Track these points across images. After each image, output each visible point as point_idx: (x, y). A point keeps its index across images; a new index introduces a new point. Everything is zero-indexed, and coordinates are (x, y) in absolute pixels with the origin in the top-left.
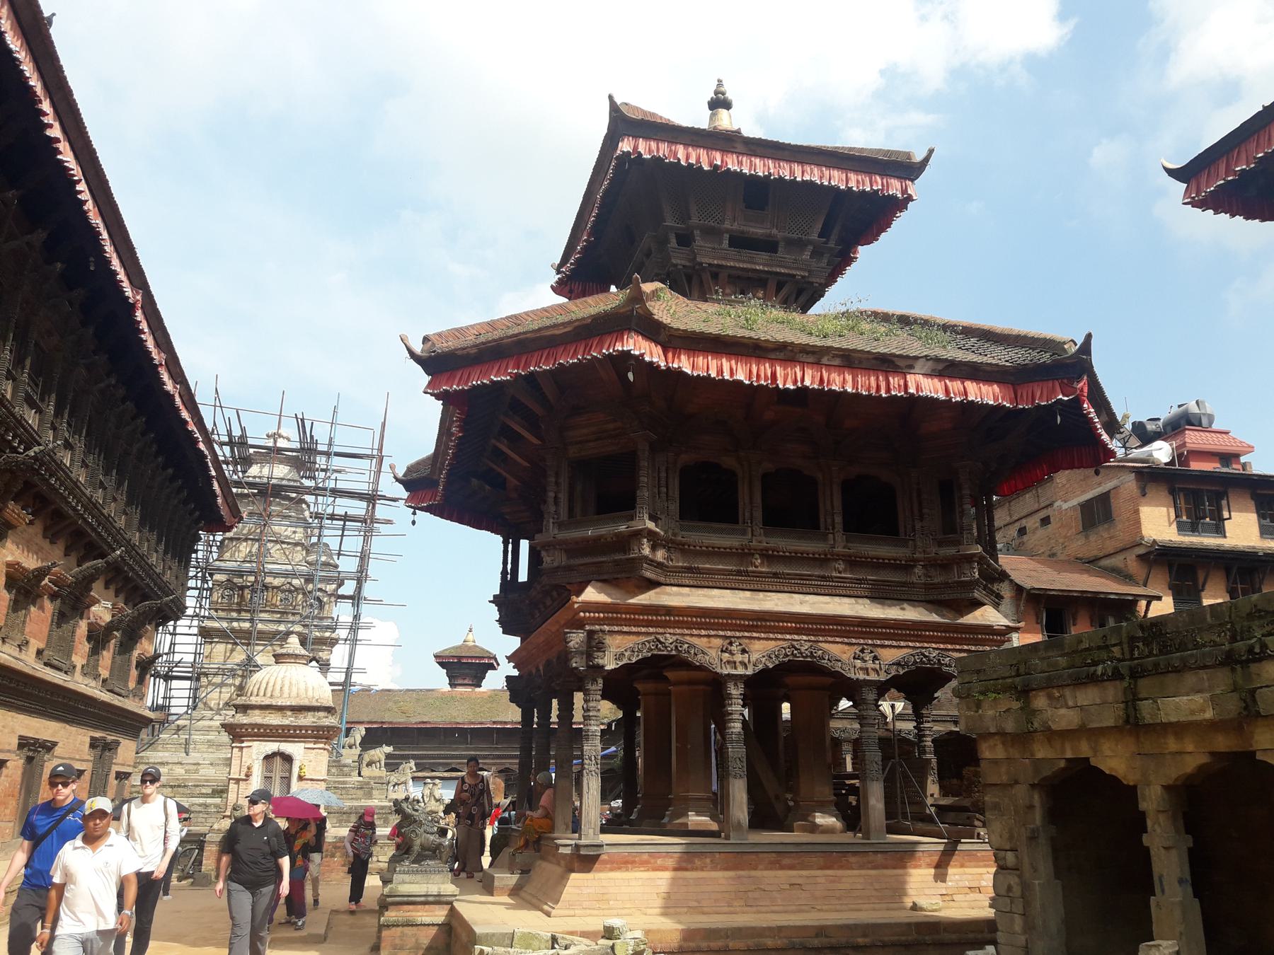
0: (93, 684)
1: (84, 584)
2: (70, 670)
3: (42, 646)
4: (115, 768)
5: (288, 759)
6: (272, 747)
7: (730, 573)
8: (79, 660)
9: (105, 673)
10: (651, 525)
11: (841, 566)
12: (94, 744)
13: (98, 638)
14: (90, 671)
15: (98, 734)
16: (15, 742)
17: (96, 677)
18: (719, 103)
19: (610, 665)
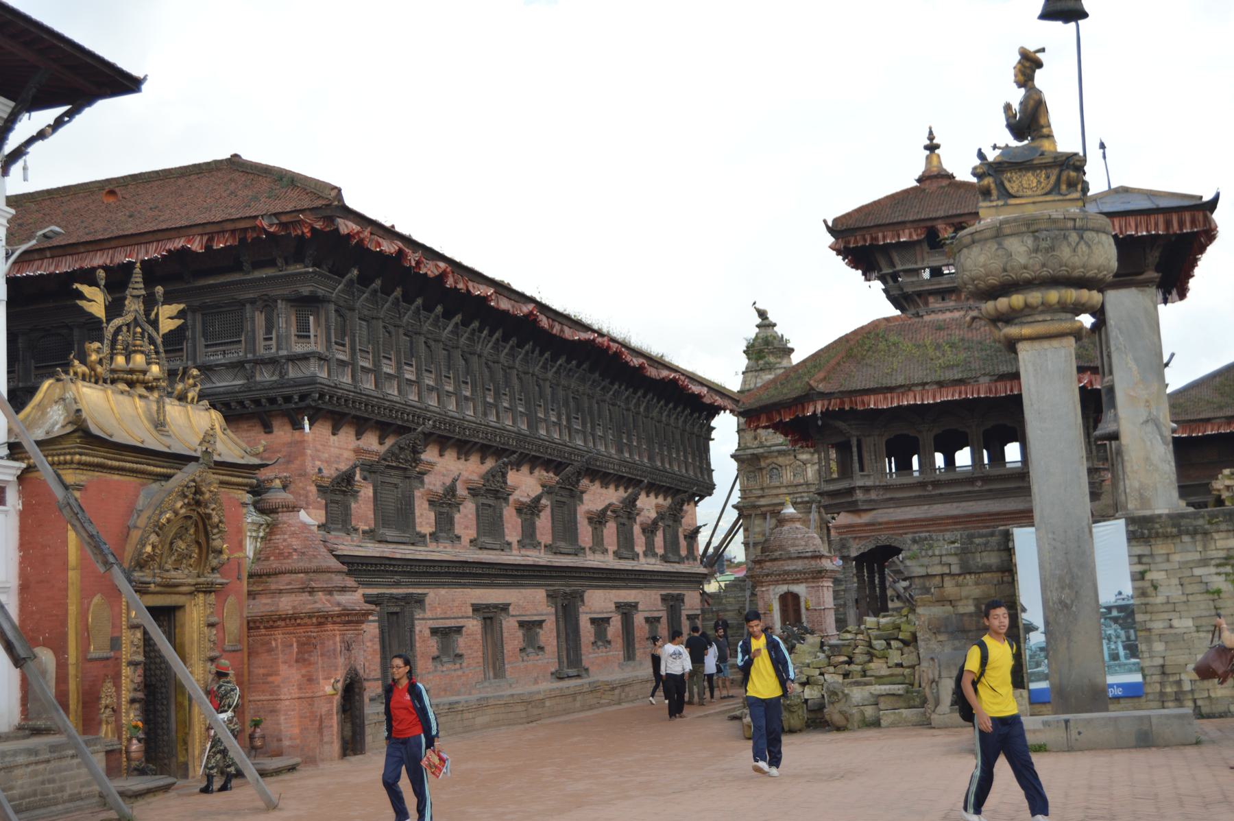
0: (653, 561)
1: (631, 503)
2: (635, 557)
3: (615, 548)
4: (684, 613)
5: (796, 597)
6: (783, 589)
7: (915, 497)
8: (640, 549)
9: (660, 551)
10: (860, 483)
11: (979, 483)
12: (664, 599)
13: (650, 530)
14: (650, 551)
15: (664, 592)
16: (613, 606)
17: (655, 555)
18: (932, 148)
19: (854, 554)
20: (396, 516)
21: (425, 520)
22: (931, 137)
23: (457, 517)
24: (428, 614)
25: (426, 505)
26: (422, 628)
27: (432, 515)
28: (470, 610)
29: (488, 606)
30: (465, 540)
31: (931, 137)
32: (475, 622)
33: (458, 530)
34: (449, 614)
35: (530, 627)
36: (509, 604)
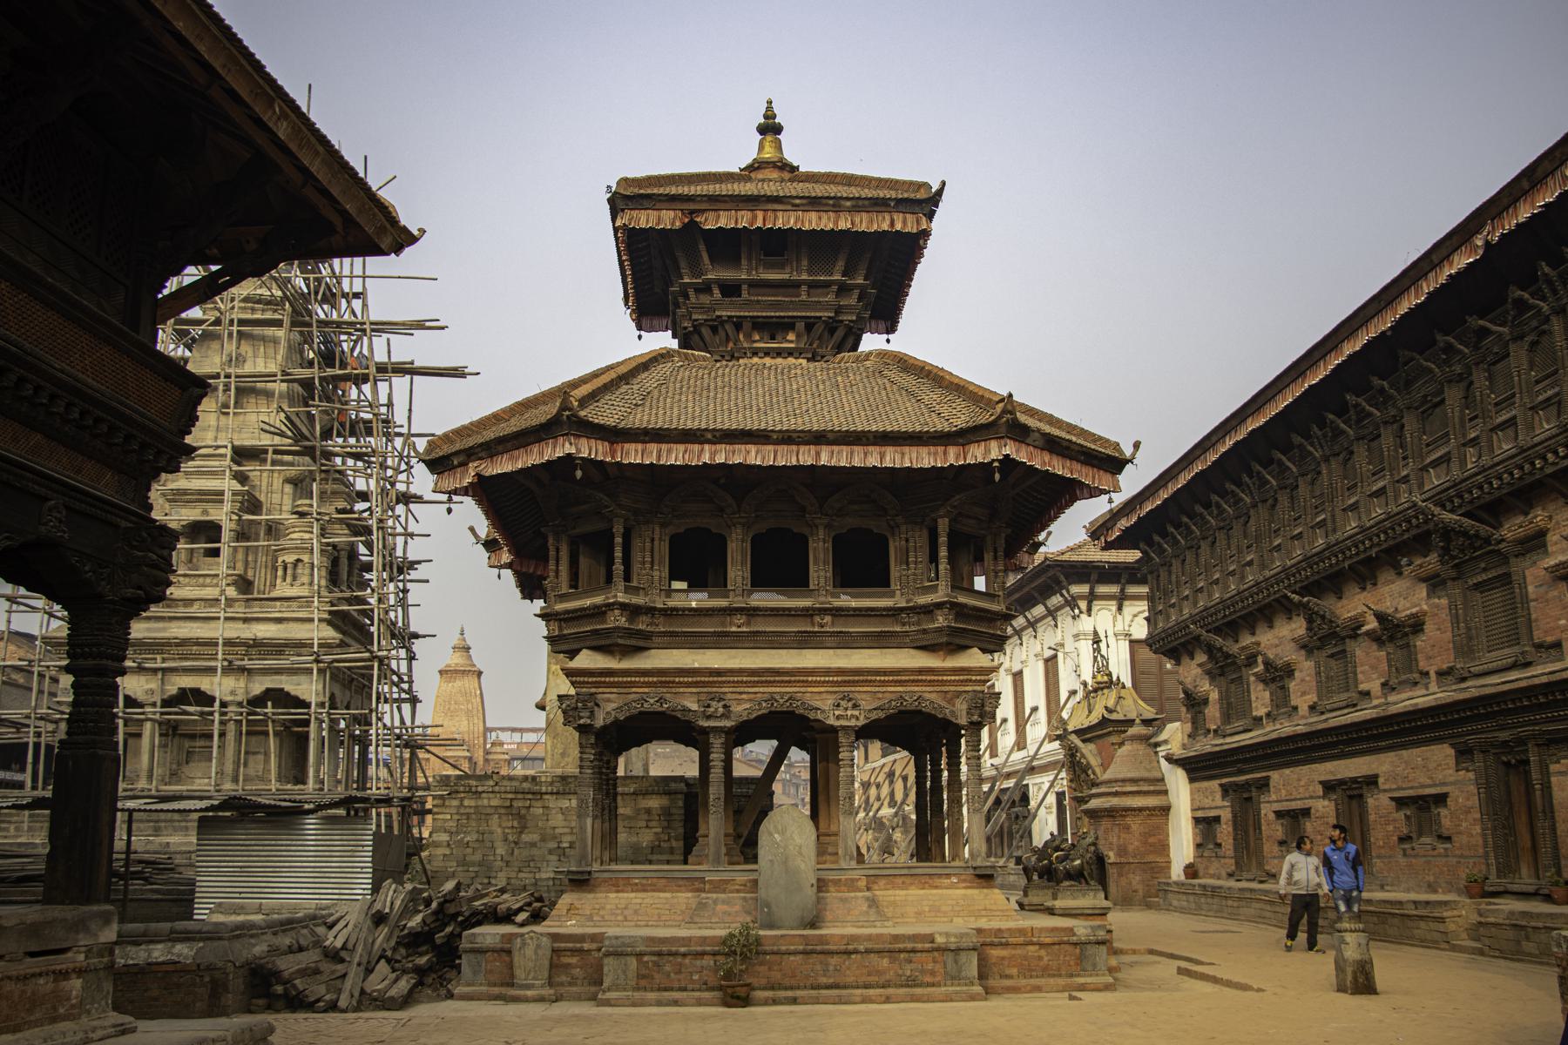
18: (770, 128)
20: (1235, 709)
21: (1261, 700)
22: (770, 115)
23: (1292, 685)
24: (1274, 797)
25: (1261, 686)
26: (1267, 811)
27: (1267, 694)
28: (1320, 790)
29: (1341, 782)
30: (1303, 709)
31: (770, 115)
32: (1326, 803)
33: (1295, 700)
34: (1295, 795)
35: (1422, 807)
36: (1376, 776)
